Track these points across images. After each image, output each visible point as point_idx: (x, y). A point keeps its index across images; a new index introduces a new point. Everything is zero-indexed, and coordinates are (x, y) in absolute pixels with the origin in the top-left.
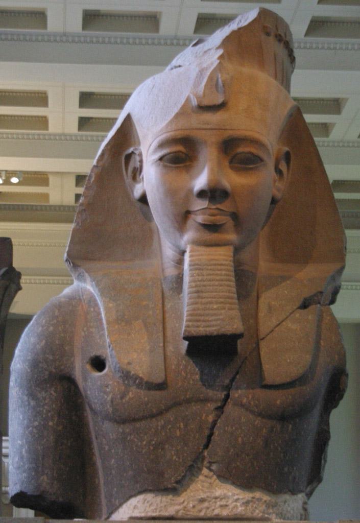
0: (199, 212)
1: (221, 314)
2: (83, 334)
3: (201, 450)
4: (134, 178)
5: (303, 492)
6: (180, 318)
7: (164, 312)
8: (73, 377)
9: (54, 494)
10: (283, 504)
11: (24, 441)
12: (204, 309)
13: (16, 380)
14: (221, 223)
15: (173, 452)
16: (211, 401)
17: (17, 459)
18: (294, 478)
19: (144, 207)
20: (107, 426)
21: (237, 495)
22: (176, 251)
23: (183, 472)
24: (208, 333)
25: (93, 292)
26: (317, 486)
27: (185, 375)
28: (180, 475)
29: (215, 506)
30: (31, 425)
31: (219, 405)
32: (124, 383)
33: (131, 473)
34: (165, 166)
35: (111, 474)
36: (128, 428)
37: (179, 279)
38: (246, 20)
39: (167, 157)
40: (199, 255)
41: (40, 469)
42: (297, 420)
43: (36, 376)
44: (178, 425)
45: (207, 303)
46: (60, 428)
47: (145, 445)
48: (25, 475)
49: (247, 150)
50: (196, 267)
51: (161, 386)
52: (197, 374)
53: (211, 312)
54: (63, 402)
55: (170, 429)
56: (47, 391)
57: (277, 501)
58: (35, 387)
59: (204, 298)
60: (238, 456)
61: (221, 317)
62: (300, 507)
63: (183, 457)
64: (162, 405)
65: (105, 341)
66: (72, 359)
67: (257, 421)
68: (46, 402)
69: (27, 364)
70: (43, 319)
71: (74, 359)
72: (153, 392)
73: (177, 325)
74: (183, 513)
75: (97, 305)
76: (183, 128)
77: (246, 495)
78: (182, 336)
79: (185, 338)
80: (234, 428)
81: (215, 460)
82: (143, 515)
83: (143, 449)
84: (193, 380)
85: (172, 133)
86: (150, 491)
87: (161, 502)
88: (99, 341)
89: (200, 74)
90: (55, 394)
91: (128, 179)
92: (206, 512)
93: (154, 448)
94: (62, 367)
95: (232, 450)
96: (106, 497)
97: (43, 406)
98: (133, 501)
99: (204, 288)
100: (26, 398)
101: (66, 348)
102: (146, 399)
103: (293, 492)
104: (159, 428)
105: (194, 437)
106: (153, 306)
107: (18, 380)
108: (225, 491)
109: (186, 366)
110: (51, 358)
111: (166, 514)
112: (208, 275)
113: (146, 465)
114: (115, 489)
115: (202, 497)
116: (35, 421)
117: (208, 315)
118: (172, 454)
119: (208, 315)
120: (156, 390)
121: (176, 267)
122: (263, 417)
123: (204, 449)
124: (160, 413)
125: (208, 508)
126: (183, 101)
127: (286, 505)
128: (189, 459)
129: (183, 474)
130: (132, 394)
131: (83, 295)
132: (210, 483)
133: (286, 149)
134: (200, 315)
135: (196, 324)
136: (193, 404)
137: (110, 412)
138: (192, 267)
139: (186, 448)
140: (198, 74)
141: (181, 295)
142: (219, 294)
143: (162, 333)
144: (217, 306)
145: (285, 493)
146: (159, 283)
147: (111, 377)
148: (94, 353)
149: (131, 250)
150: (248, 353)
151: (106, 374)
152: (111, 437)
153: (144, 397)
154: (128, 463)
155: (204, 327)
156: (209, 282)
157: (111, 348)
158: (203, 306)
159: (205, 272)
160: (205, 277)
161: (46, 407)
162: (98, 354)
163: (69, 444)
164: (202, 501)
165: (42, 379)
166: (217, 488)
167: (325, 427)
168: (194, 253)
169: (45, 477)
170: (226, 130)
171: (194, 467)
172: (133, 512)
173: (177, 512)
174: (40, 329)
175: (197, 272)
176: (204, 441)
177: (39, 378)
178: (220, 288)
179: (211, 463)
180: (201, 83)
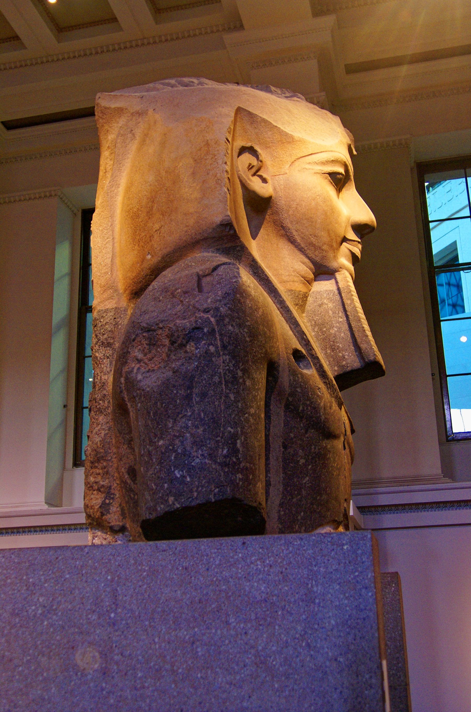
13: (224, 347)
17: (225, 451)
22: (310, 269)
114: (302, 514)
152: (313, 450)
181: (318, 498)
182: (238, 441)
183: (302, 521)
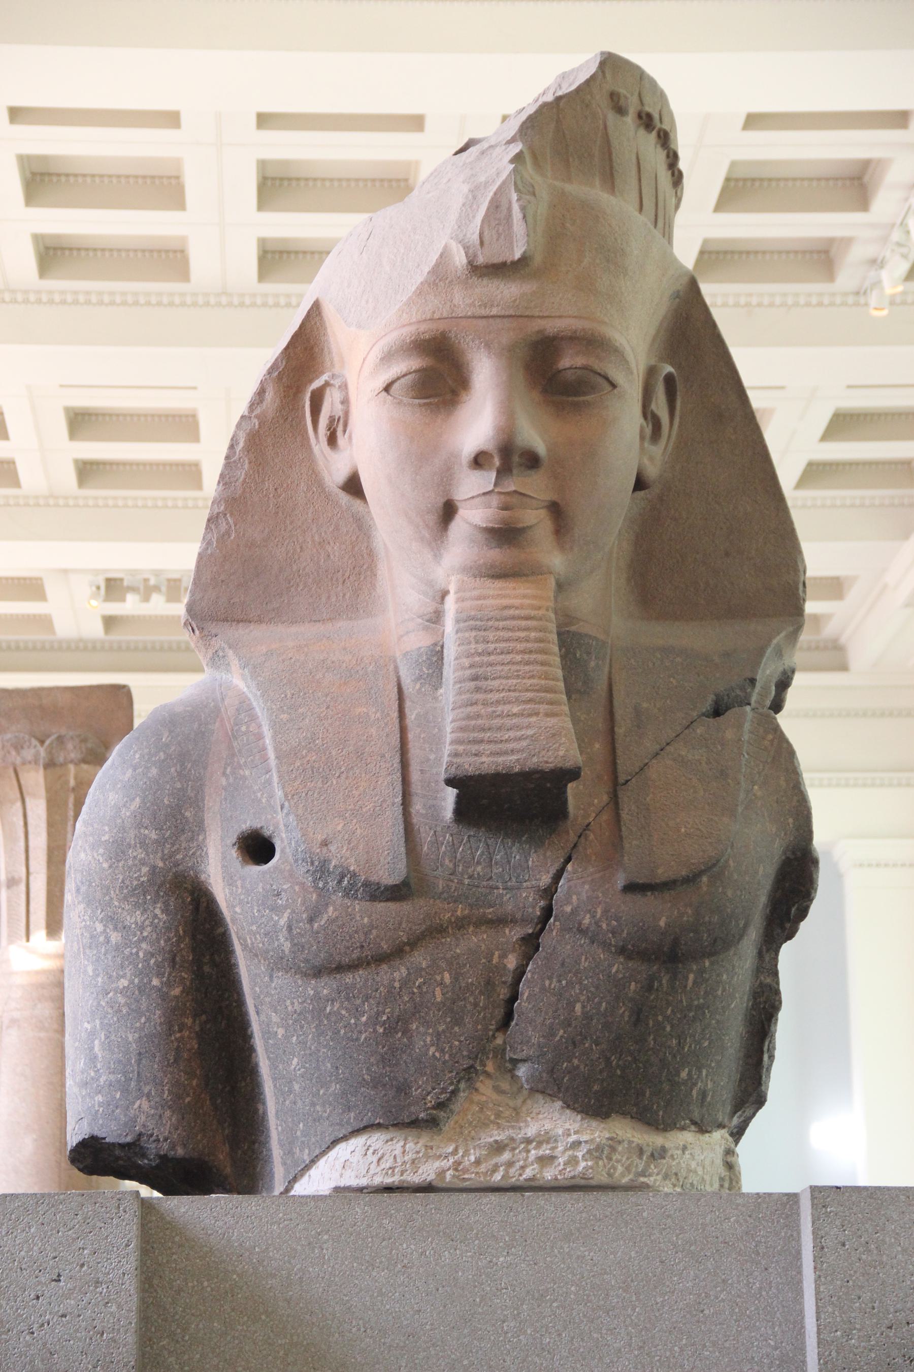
0: (477, 500)
1: (528, 727)
2: (224, 781)
3: (491, 1033)
4: (332, 440)
5: (724, 1127)
6: (436, 741)
7: (403, 730)
8: (203, 877)
9: (166, 1140)
10: (680, 1152)
11: (98, 1022)
12: (492, 716)
13: (78, 890)
14: (525, 525)
15: (429, 1039)
16: (511, 921)
18: (703, 1094)
19: (357, 503)
20: (281, 980)
21: (576, 1133)
23: (452, 1084)
24: (500, 768)
25: (245, 690)
26: (754, 1115)
27: (451, 865)
28: (444, 1091)
29: (526, 1160)
30: (114, 985)
31: (530, 931)
32: (316, 887)
33: (335, 1088)
34: (400, 403)
35: (290, 1091)
36: (326, 986)
37: (437, 655)
38: (570, 85)
39: (403, 380)
40: (479, 598)
41: (133, 1084)
42: (707, 964)
43: (121, 877)
44: (438, 978)
45: (498, 702)
46: (177, 991)
47: (366, 1024)
48: (99, 1098)
49: (580, 361)
50: (472, 623)
51: (397, 893)
52: (478, 863)
53: (509, 722)
54: (181, 932)
55: (419, 987)
56: (145, 910)
57: (668, 1145)
58: (119, 900)
59: (491, 691)
60: (574, 1044)
61: (530, 732)
62: (719, 1162)
63: (451, 1047)
64: (402, 934)
65: (271, 796)
66: (201, 838)
67: (616, 966)
68: (145, 934)
69: (101, 851)
70: (135, 752)
71: (205, 839)
72: (380, 906)
73: (432, 757)
74: (454, 1176)
75: (253, 718)
76: (436, 316)
77: (595, 1132)
78: (443, 776)
79: (450, 782)
80: (564, 982)
81: (523, 1055)
82: (363, 1182)
83: (360, 1032)
84: (470, 877)
85: (413, 329)
86: (379, 1126)
87: (404, 1152)
88: (259, 795)
89: (470, 197)
90: (164, 917)
91: (319, 445)
92: (507, 1172)
93: (385, 1028)
94: (179, 857)
95: (561, 1032)
96: (281, 1145)
97: (140, 941)
98: (342, 1151)
99: (489, 669)
100: (99, 927)
101: (187, 814)
102: (366, 920)
103: (702, 1128)
104: (397, 985)
105: (476, 1005)
106: (378, 715)
107: (83, 889)
108: (548, 1126)
109: (453, 847)
110: (154, 835)
111: (415, 1179)
112: (498, 641)
113: (368, 1069)
114: (301, 1125)
115: (498, 1138)
116: (119, 977)
117: (499, 729)
118: (424, 1041)
119: (499, 729)
120: (387, 900)
121: (426, 628)
122: (629, 958)
123: (498, 1030)
124: (398, 952)
125: (510, 1164)
126: (434, 258)
127: (687, 1155)
128: (465, 1053)
129: (451, 1088)
130: (335, 910)
131: (223, 699)
132: (515, 1109)
133: (669, 369)
134: (483, 730)
135: (474, 748)
136: (471, 929)
137: (287, 952)
138: (462, 625)
139: (456, 1029)
140: (467, 197)
141: (441, 691)
142: (524, 681)
143: (399, 774)
144: (520, 708)
145: (683, 1128)
146: (391, 668)
147: (286, 874)
148: (247, 823)
149: (329, 597)
150: (594, 815)
151: (275, 867)
152: (290, 1008)
153: (362, 918)
154: (329, 1065)
155: (492, 754)
156: (503, 657)
157: (285, 811)
158: (490, 709)
159: (491, 635)
160: (491, 647)
161: (144, 945)
162: (257, 824)
163: (197, 1028)
164: (498, 1148)
165: (135, 883)
166: (529, 1119)
167: (768, 980)
168: (468, 594)
169: (145, 1105)
170: (533, 316)
171: (476, 1071)
172: (341, 1176)
173: (441, 1173)
174: (129, 773)
175: (474, 633)
176: (499, 1013)
177: (127, 882)
178: (527, 668)
179: (515, 1062)
180: (474, 217)
181: (321, 1092)
182: (96, 1042)
183: (303, 1139)
